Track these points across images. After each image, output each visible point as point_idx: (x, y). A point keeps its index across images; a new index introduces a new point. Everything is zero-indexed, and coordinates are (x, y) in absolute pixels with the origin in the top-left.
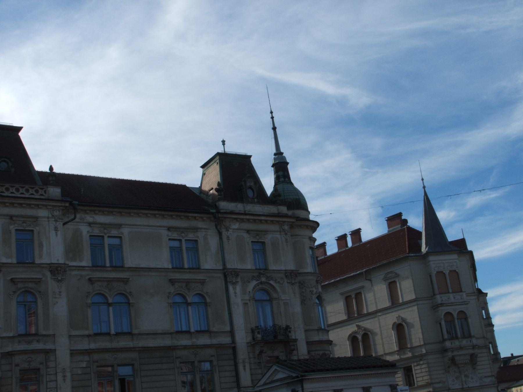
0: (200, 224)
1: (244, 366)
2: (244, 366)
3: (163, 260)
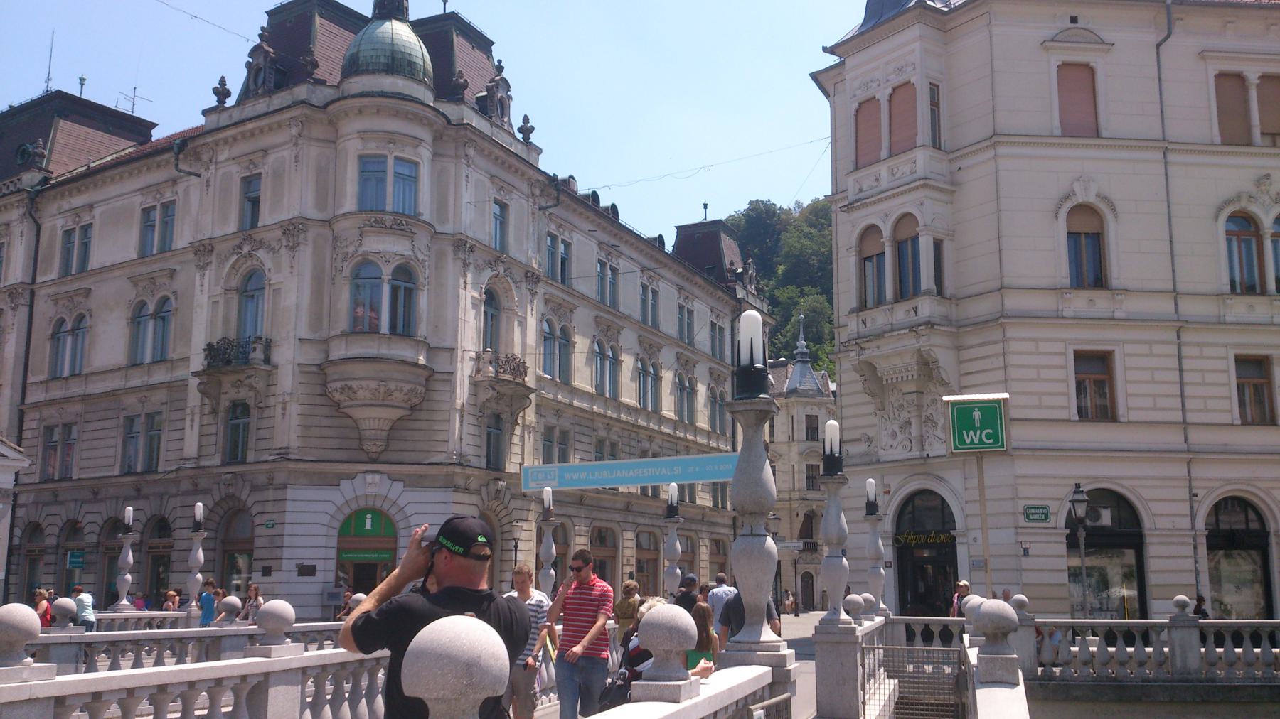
1: (192, 421)
2: (192, 421)
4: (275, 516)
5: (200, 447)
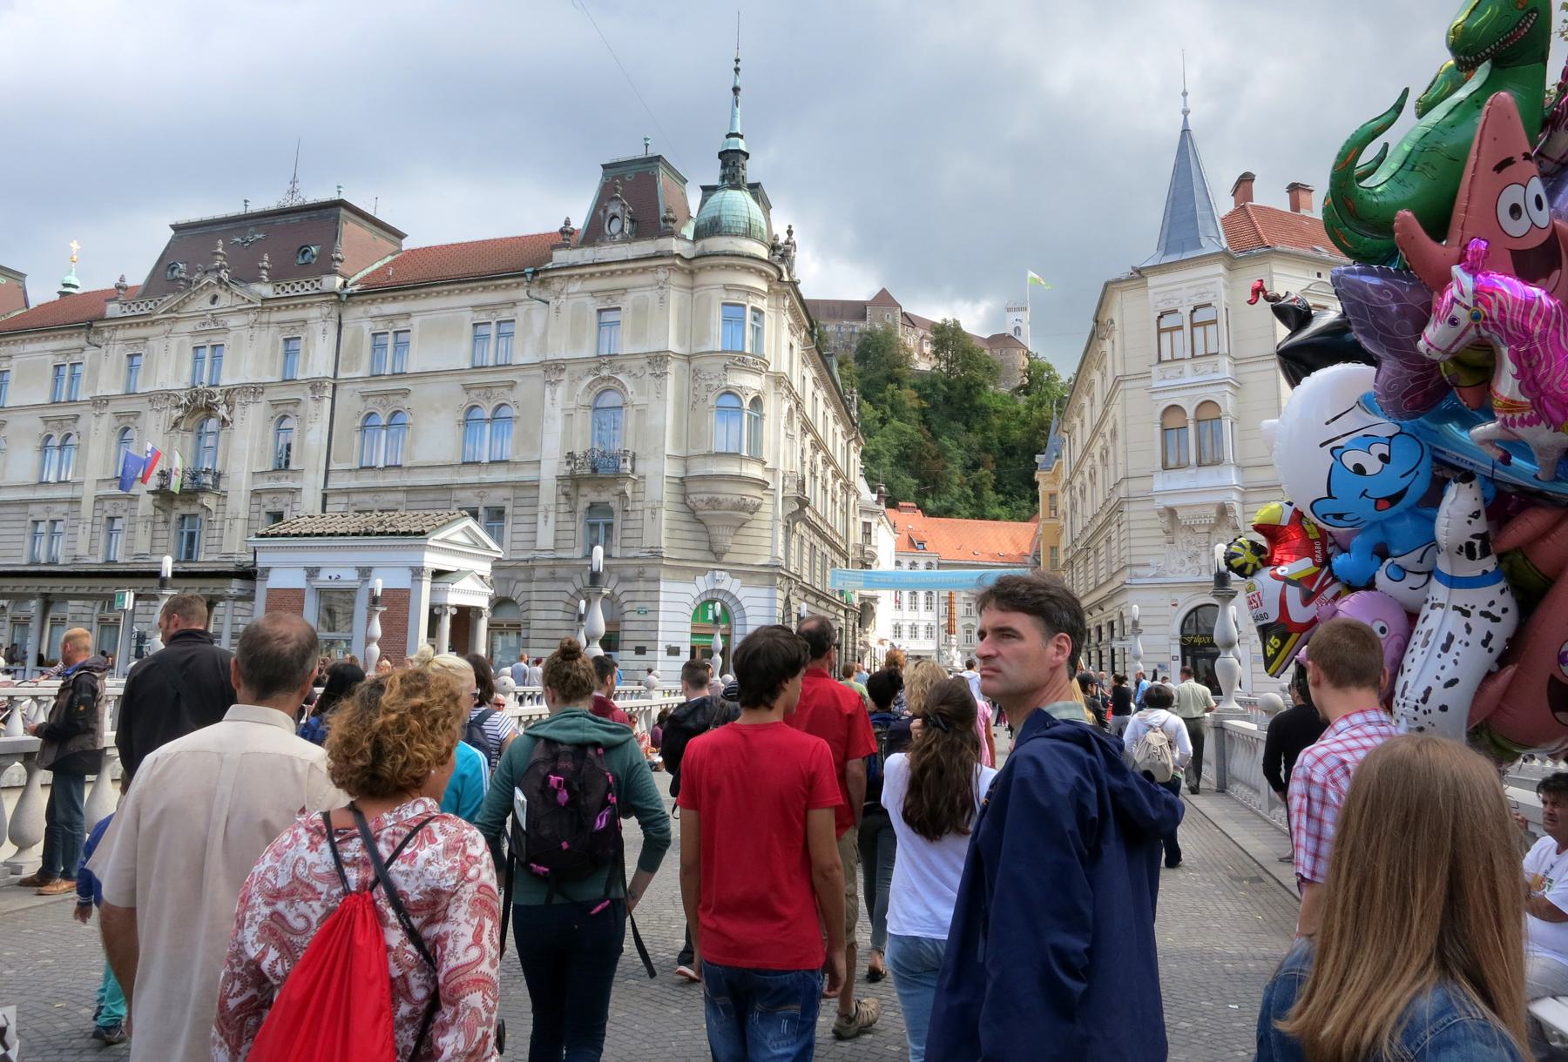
0: (521, 294)
3: (459, 357)
4: (648, 605)
5: (556, 540)
